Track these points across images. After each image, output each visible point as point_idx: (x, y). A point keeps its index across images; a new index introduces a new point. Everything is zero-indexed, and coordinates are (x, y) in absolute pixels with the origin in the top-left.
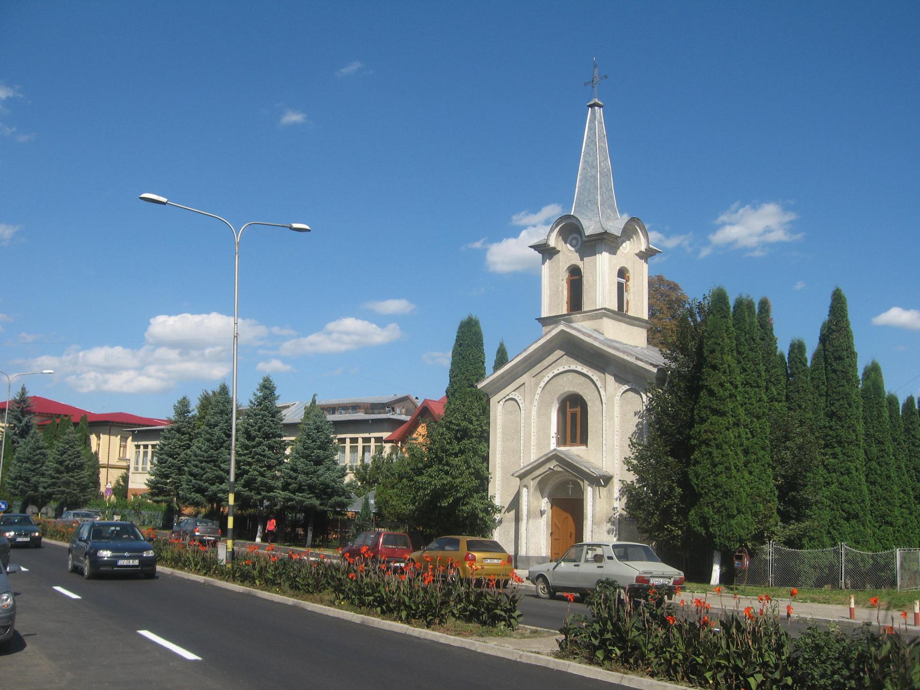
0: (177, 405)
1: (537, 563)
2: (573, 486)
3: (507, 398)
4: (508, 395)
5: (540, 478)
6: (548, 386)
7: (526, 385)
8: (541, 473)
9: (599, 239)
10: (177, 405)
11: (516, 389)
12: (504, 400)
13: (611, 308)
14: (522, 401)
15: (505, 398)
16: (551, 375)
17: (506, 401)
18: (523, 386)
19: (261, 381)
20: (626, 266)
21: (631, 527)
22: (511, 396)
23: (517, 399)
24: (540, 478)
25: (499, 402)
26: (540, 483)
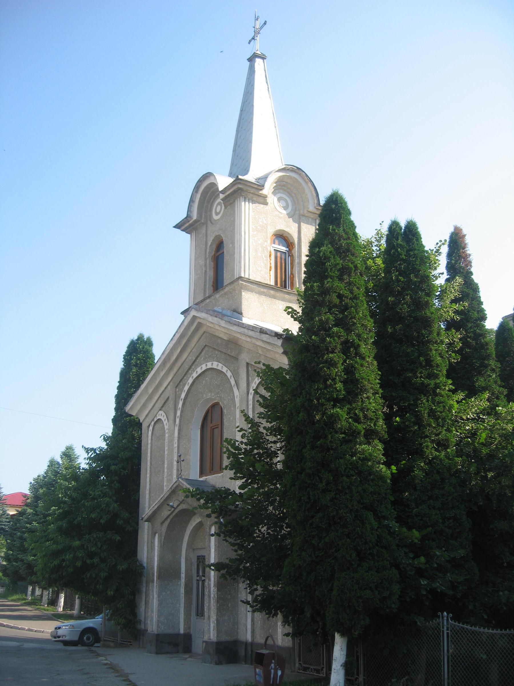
0: (33, 482)
3: (155, 420)
4: (156, 416)
5: (169, 520)
7: (170, 399)
9: (235, 192)
10: (33, 482)
12: (153, 423)
13: (262, 281)
15: (153, 420)
16: (190, 381)
17: (155, 424)
19: (63, 449)
20: (286, 230)
24: (169, 520)
26: (169, 527)
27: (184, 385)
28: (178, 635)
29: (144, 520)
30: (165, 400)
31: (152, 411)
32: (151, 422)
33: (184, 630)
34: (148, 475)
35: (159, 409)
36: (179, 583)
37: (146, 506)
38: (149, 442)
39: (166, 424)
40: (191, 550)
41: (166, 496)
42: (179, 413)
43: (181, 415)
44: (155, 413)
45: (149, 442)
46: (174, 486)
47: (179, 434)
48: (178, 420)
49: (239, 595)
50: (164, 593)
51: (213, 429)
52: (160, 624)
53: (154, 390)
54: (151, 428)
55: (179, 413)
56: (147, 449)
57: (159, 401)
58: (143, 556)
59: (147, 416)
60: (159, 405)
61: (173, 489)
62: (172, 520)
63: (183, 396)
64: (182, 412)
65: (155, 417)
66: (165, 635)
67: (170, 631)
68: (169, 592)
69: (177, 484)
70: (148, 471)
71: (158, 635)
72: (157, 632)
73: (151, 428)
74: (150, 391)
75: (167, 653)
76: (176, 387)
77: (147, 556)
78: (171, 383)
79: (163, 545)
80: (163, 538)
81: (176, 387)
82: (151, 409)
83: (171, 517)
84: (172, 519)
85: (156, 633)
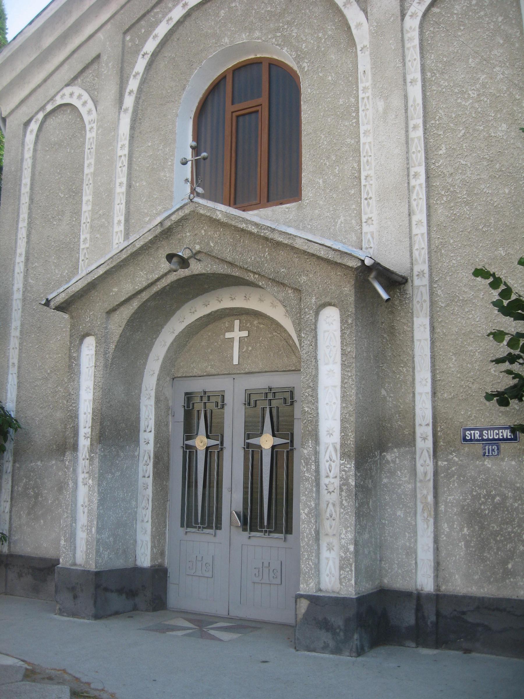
1: (120, 591)
2: (245, 334)
3: (49, 108)
4: (52, 99)
5: (135, 304)
6: (167, 53)
7: (104, 58)
8: (138, 288)
11: (75, 78)
12: (41, 116)
14: (90, 104)
15: (43, 108)
17: (46, 117)
18: (95, 66)
21: (488, 463)
22: (59, 101)
23: (78, 104)
25: (27, 124)
27: (157, 23)
28: (137, 570)
29: (52, 304)
30: (87, 62)
31: (41, 90)
32: (37, 113)
33: (151, 561)
34: (23, 224)
35: (66, 82)
36: (136, 454)
37: (15, 288)
38: (28, 155)
39: (89, 112)
40: (168, 379)
41: (138, 245)
42: (133, 84)
43: (140, 90)
44: (52, 92)
45: (28, 155)
46: (174, 218)
47: (133, 128)
48: (129, 101)
49: (385, 481)
50: (110, 476)
51: (238, 117)
52: (101, 549)
53: (57, 39)
54: (34, 126)
55: (133, 84)
56: (20, 169)
57: (66, 67)
58: (6, 396)
59: (22, 102)
60: (66, 73)
61: (168, 224)
62: (143, 307)
63: (150, 46)
64: (143, 82)
65: (48, 102)
66: (111, 572)
67: (120, 563)
68: (118, 474)
69: (187, 211)
70: (24, 214)
71: (98, 574)
72: (96, 567)
73: (34, 126)
74: (48, 41)
75: (116, 613)
76: (125, 33)
77: (18, 395)
78: (109, 26)
79: (112, 364)
80: (113, 346)
81: (125, 33)
82: (39, 86)
83: (145, 296)
84: (147, 301)
85: (93, 567)
